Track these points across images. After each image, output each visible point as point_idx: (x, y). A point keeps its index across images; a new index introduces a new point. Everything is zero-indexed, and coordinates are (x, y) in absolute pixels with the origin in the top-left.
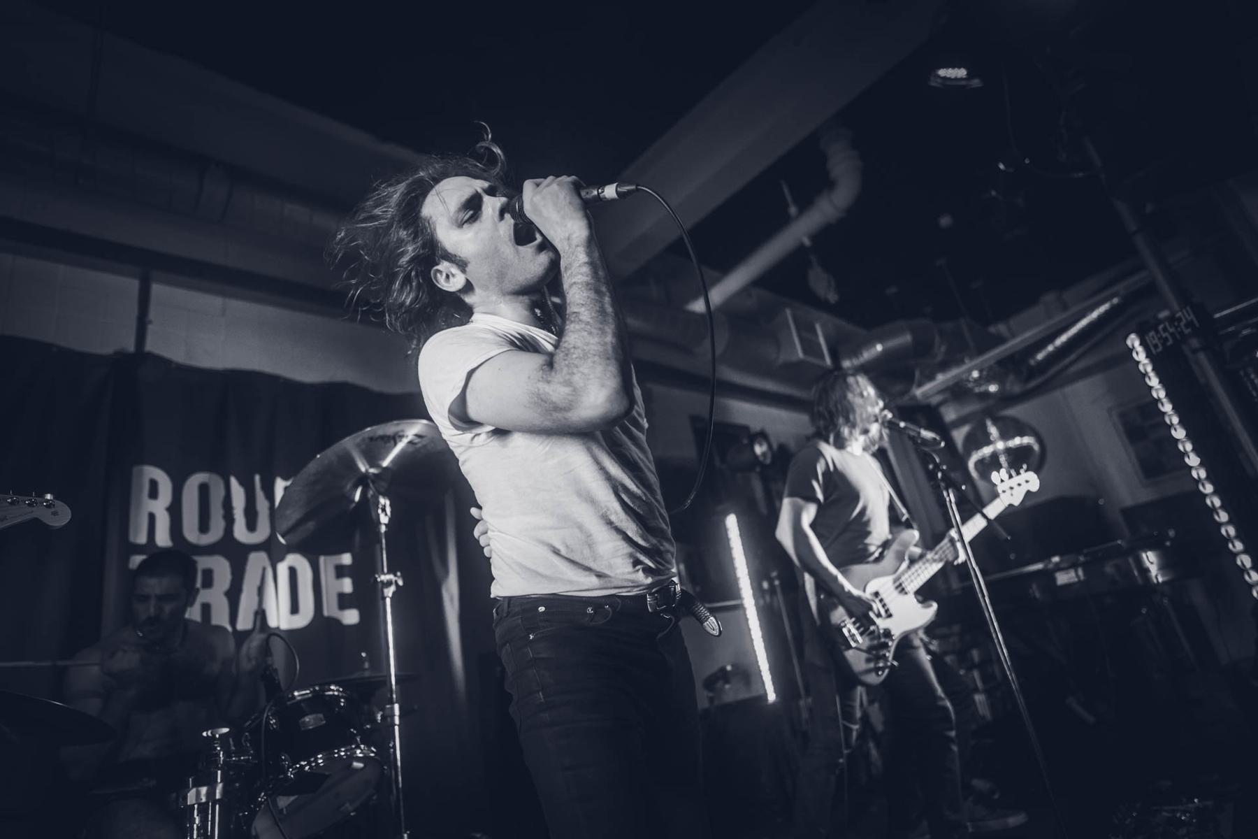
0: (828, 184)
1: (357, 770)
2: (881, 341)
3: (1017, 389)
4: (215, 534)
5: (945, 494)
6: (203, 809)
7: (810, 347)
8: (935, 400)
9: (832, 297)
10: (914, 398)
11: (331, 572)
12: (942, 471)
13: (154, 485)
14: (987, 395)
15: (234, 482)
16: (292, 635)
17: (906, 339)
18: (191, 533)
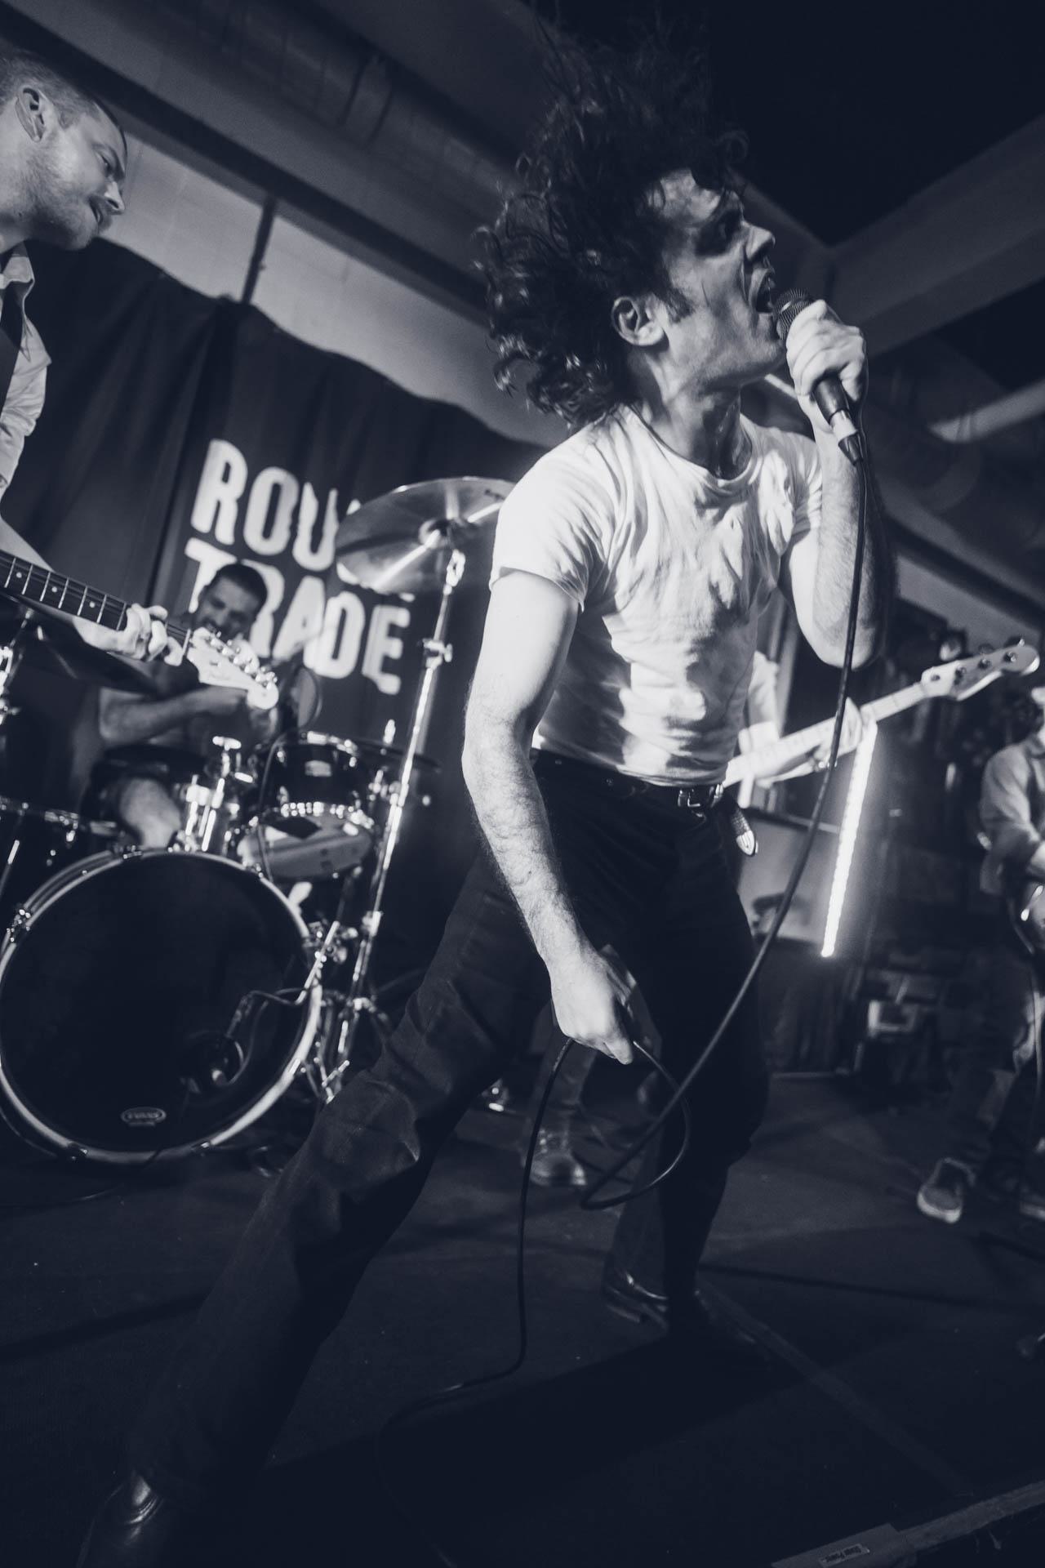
4: (275, 545)
13: (228, 468)
15: (308, 490)
18: (253, 536)
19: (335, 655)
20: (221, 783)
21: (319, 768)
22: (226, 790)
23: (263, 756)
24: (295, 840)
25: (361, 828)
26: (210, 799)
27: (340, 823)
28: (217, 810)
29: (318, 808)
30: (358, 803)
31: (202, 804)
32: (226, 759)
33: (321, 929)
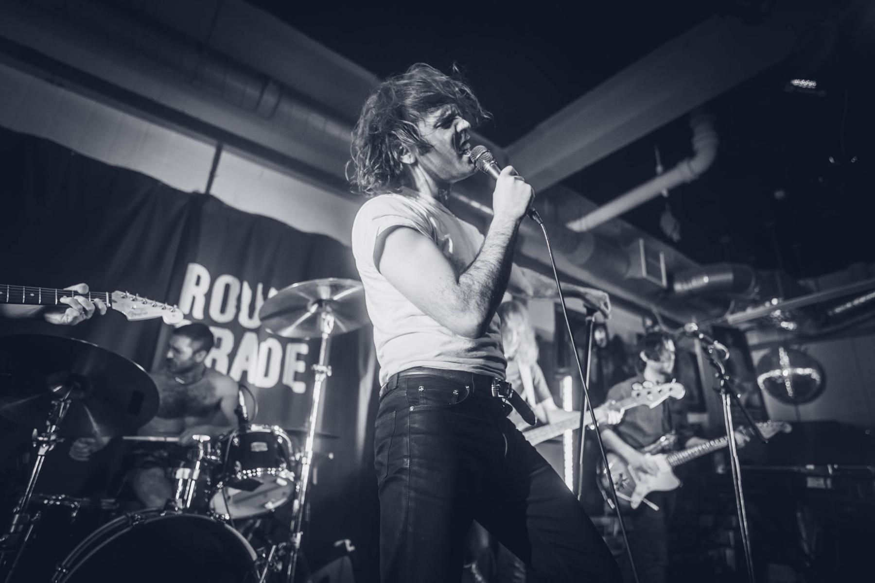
0: (689, 154)
1: (279, 486)
2: (709, 274)
3: (812, 331)
4: (228, 317)
5: (724, 396)
6: (185, 482)
7: (653, 269)
8: (743, 327)
9: (676, 237)
10: (726, 321)
11: (294, 356)
12: (725, 380)
13: (199, 278)
14: (784, 331)
15: (246, 285)
16: (263, 391)
17: (728, 277)
19: (266, 374)
20: (198, 464)
21: (259, 447)
22: (202, 468)
23: (225, 443)
24: (247, 493)
25: (287, 479)
27: (274, 478)
28: (195, 480)
29: (259, 471)
30: (284, 465)
31: (186, 477)
32: (201, 447)
33: (265, 551)
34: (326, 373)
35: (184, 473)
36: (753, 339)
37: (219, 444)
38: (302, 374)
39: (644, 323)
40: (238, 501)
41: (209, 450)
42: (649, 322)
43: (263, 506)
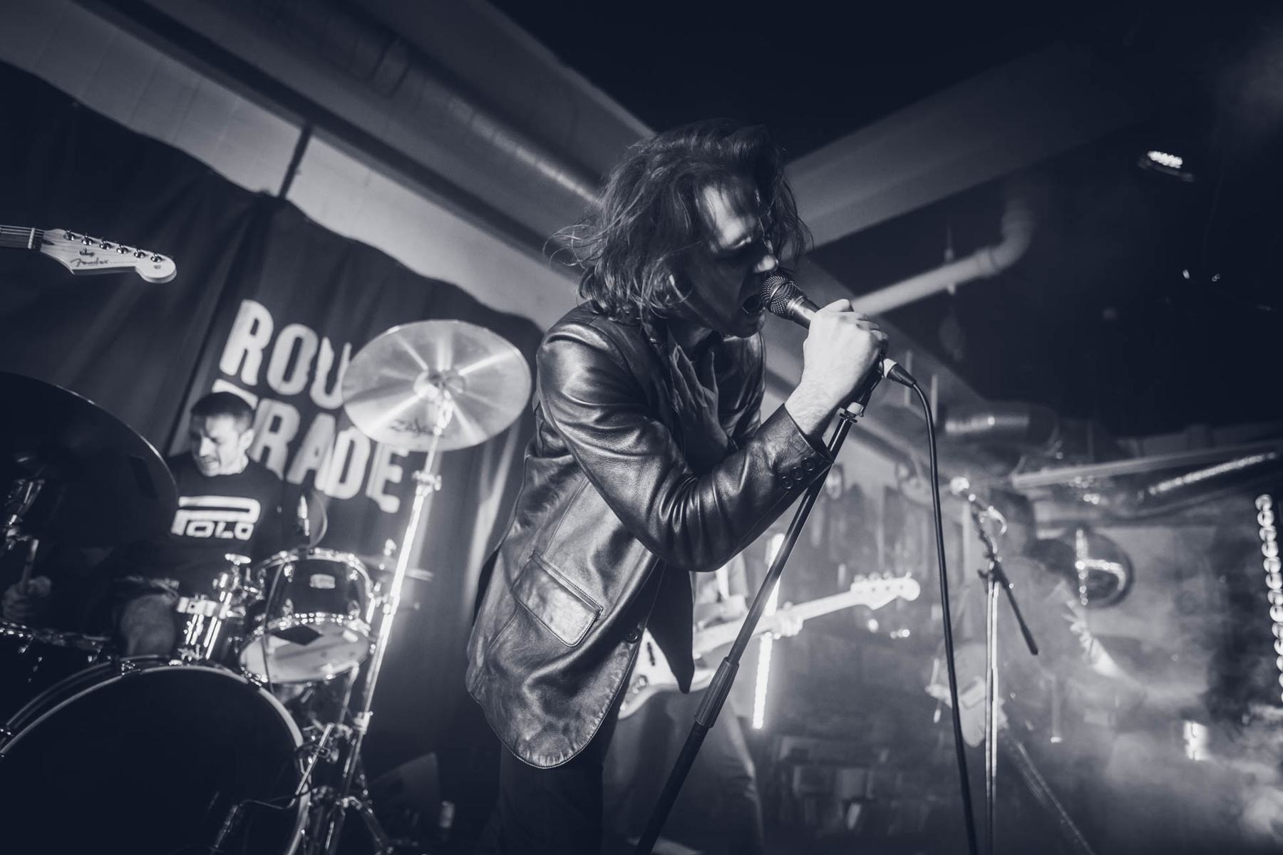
0: (993, 239)
1: (346, 642)
2: (996, 412)
3: (1124, 512)
6: (207, 621)
8: (1032, 494)
11: (386, 458)
13: (256, 323)
15: (326, 343)
19: (343, 479)
21: (322, 581)
25: (359, 634)
26: (216, 613)
29: (320, 617)
31: (209, 614)
34: (433, 486)
35: (206, 607)
36: (1044, 513)
37: (264, 571)
38: (396, 485)
39: (897, 472)
40: (282, 657)
41: (248, 578)
42: (904, 472)
43: (317, 669)
